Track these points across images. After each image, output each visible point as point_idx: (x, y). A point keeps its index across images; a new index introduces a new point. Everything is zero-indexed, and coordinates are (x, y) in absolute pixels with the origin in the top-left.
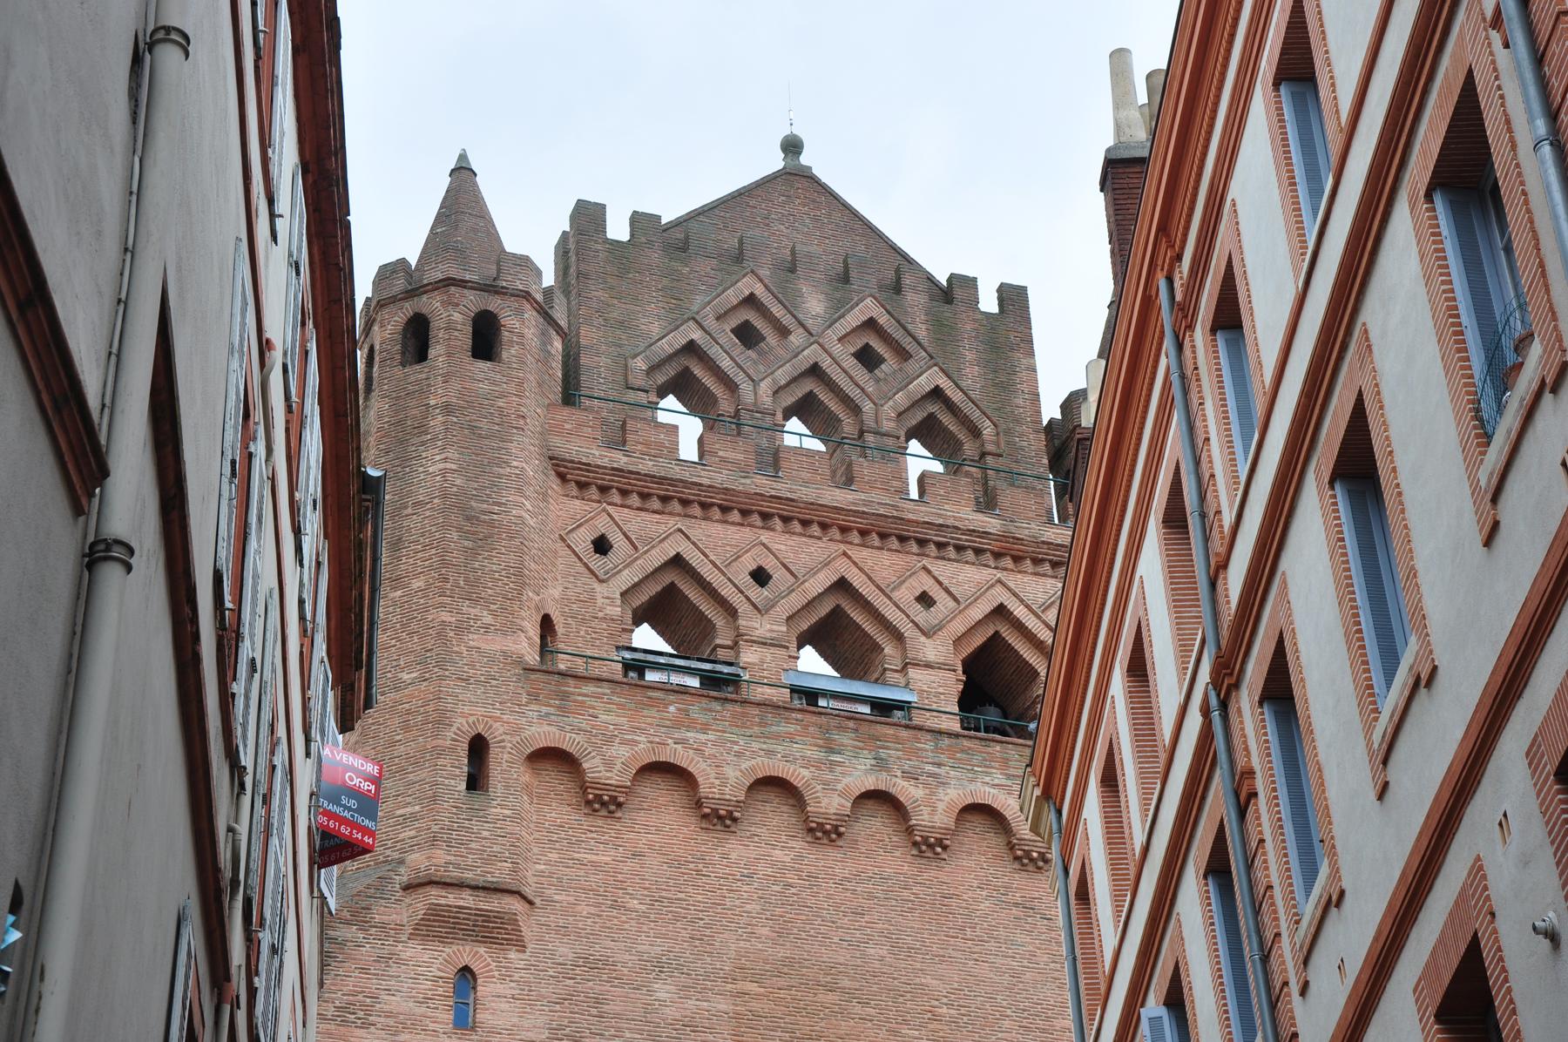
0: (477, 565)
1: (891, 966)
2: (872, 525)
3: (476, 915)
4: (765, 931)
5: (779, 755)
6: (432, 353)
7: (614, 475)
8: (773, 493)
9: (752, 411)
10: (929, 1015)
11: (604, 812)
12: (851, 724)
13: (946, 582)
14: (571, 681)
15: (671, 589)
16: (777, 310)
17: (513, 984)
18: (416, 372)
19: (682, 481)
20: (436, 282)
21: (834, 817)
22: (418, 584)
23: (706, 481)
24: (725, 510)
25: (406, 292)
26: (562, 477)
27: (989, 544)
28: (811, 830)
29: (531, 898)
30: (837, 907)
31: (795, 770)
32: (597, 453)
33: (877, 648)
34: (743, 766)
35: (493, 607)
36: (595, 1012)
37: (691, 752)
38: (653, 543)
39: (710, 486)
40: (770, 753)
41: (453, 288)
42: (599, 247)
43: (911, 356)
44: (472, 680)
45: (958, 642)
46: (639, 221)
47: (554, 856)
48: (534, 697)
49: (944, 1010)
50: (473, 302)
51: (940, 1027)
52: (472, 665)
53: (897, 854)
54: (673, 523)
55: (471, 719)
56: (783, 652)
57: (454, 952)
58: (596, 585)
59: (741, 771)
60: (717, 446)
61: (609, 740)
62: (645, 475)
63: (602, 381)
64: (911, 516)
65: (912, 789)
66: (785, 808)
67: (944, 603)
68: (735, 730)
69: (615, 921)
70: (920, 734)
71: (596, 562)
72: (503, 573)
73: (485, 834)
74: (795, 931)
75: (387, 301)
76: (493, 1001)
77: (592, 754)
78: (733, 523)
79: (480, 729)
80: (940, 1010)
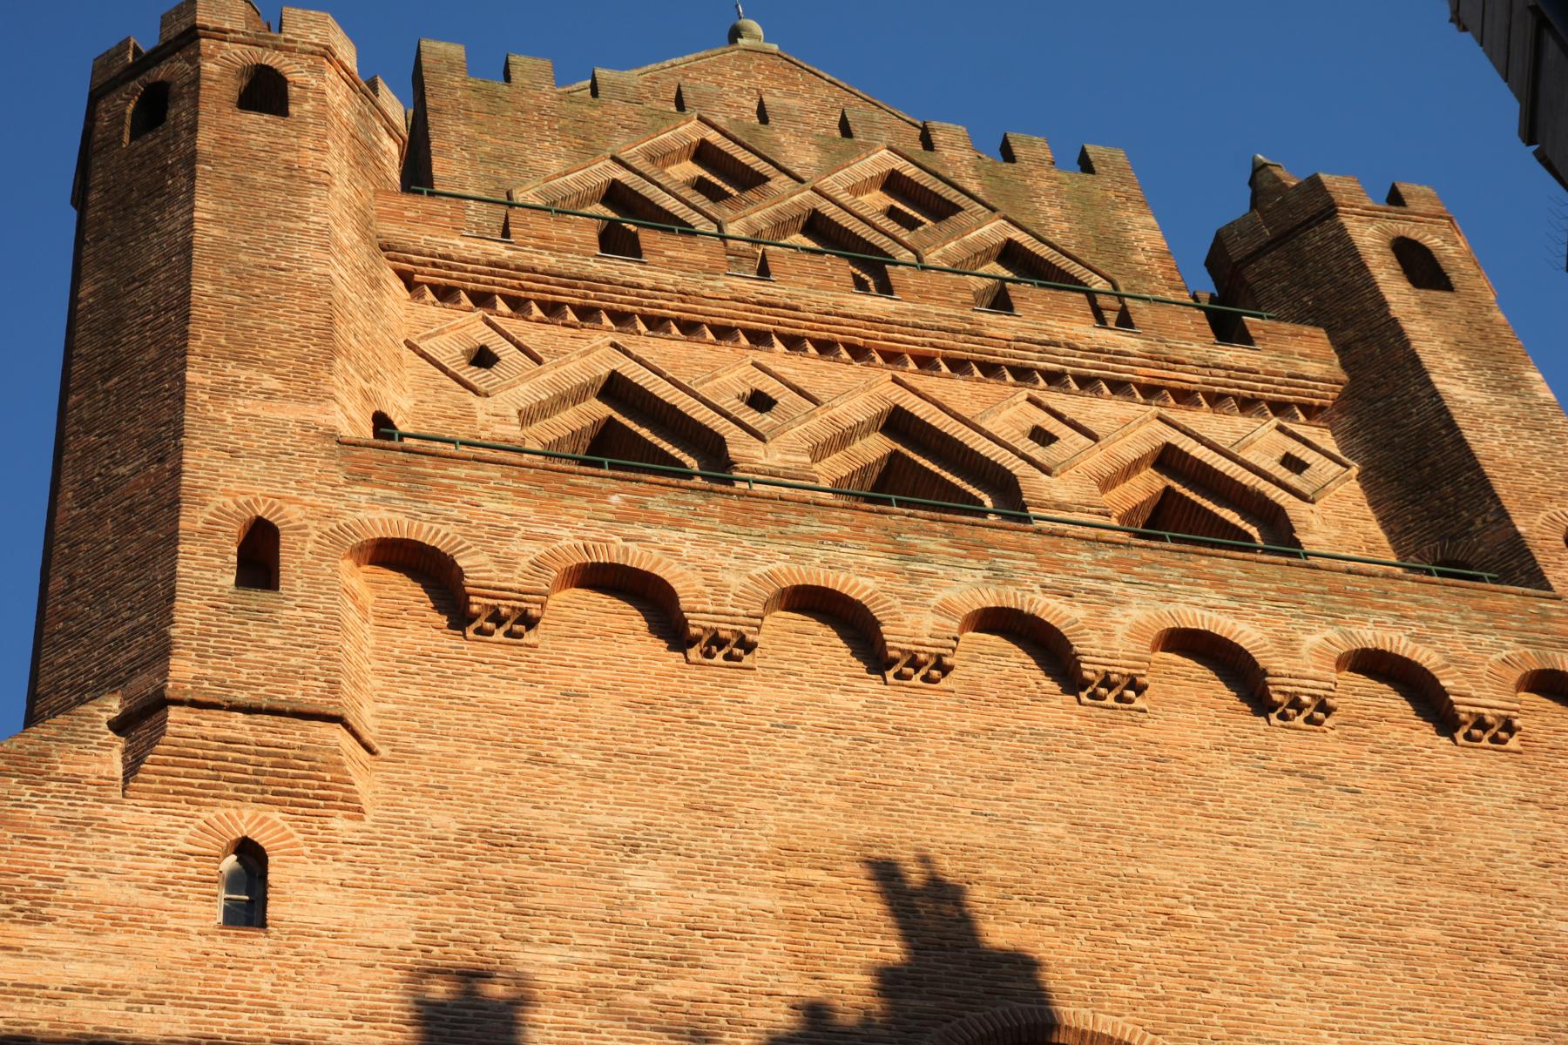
1: (1076, 850)
2: (932, 345)
3: (257, 753)
4: (829, 799)
5: (817, 561)
7: (492, 274)
8: (762, 297)
13: (1070, 415)
14: (425, 459)
17: (338, 865)
21: (933, 641)
31: (848, 579)
34: (753, 573)
36: (510, 906)
47: (413, 692)
49: (1190, 911)
52: (244, 434)
55: (242, 499)
61: (506, 533)
73: (272, 642)
74: (885, 799)
77: (474, 549)
79: (261, 511)
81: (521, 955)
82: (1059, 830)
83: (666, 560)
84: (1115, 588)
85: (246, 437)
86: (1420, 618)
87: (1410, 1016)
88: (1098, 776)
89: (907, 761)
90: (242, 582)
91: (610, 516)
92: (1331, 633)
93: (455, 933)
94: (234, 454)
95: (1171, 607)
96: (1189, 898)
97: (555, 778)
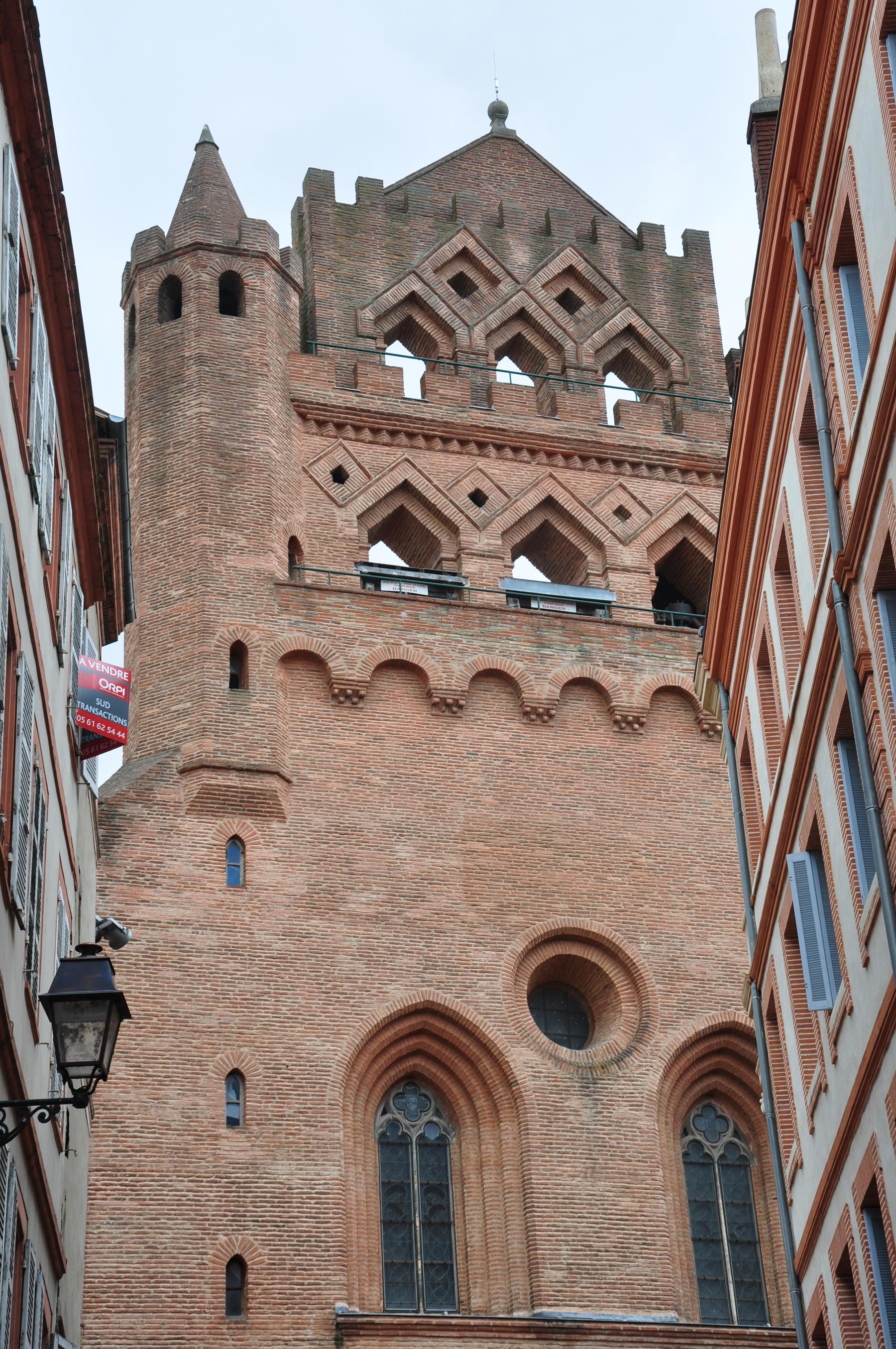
0: (231, 495)
3: (242, 792)
4: (489, 799)
6: (185, 310)
7: (348, 413)
9: (468, 353)
10: (631, 864)
11: (348, 704)
12: (559, 622)
13: (639, 497)
14: (316, 594)
15: (401, 512)
16: (488, 262)
17: (276, 849)
18: (172, 328)
19: (407, 417)
20: (186, 247)
22: (181, 514)
23: (428, 416)
24: (446, 440)
25: (161, 256)
26: (303, 417)
27: (677, 462)
28: (526, 714)
29: (288, 777)
30: (550, 777)
31: (511, 663)
32: (332, 394)
33: (581, 556)
34: (466, 661)
35: (246, 531)
37: (421, 650)
38: (383, 472)
39: (432, 421)
40: (489, 649)
41: (200, 252)
42: (329, 210)
43: (607, 299)
44: (231, 595)
45: (651, 548)
46: (364, 186)
47: (306, 742)
48: (285, 608)
49: (644, 860)
50: (218, 263)
51: (639, 873)
53: (601, 731)
54: (401, 453)
55: (231, 628)
56: (500, 562)
57: (225, 824)
58: (336, 510)
59: (465, 665)
60: (437, 385)
61: (350, 642)
62: (375, 413)
63: (335, 330)
64: (608, 441)
65: (612, 676)
66: (504, 696)
67: (638, 515)
68: (459, 630)
69: (361, 795)
70: (618, 629)
71: (335, 490)
72: (254, 502)
73: (247, 724)
74: (515, 798)
75: (144, 265)
76: (260, 863)
77: (337, 655)
78: (453, 452)
79: (239, 636)
80: (640, 860)
81: (351, 898)
83: (426, 656)
85: (232, 584)
87: (730, 916)
91: (401, 626)
96: (644, 851)
97: (368, 792)
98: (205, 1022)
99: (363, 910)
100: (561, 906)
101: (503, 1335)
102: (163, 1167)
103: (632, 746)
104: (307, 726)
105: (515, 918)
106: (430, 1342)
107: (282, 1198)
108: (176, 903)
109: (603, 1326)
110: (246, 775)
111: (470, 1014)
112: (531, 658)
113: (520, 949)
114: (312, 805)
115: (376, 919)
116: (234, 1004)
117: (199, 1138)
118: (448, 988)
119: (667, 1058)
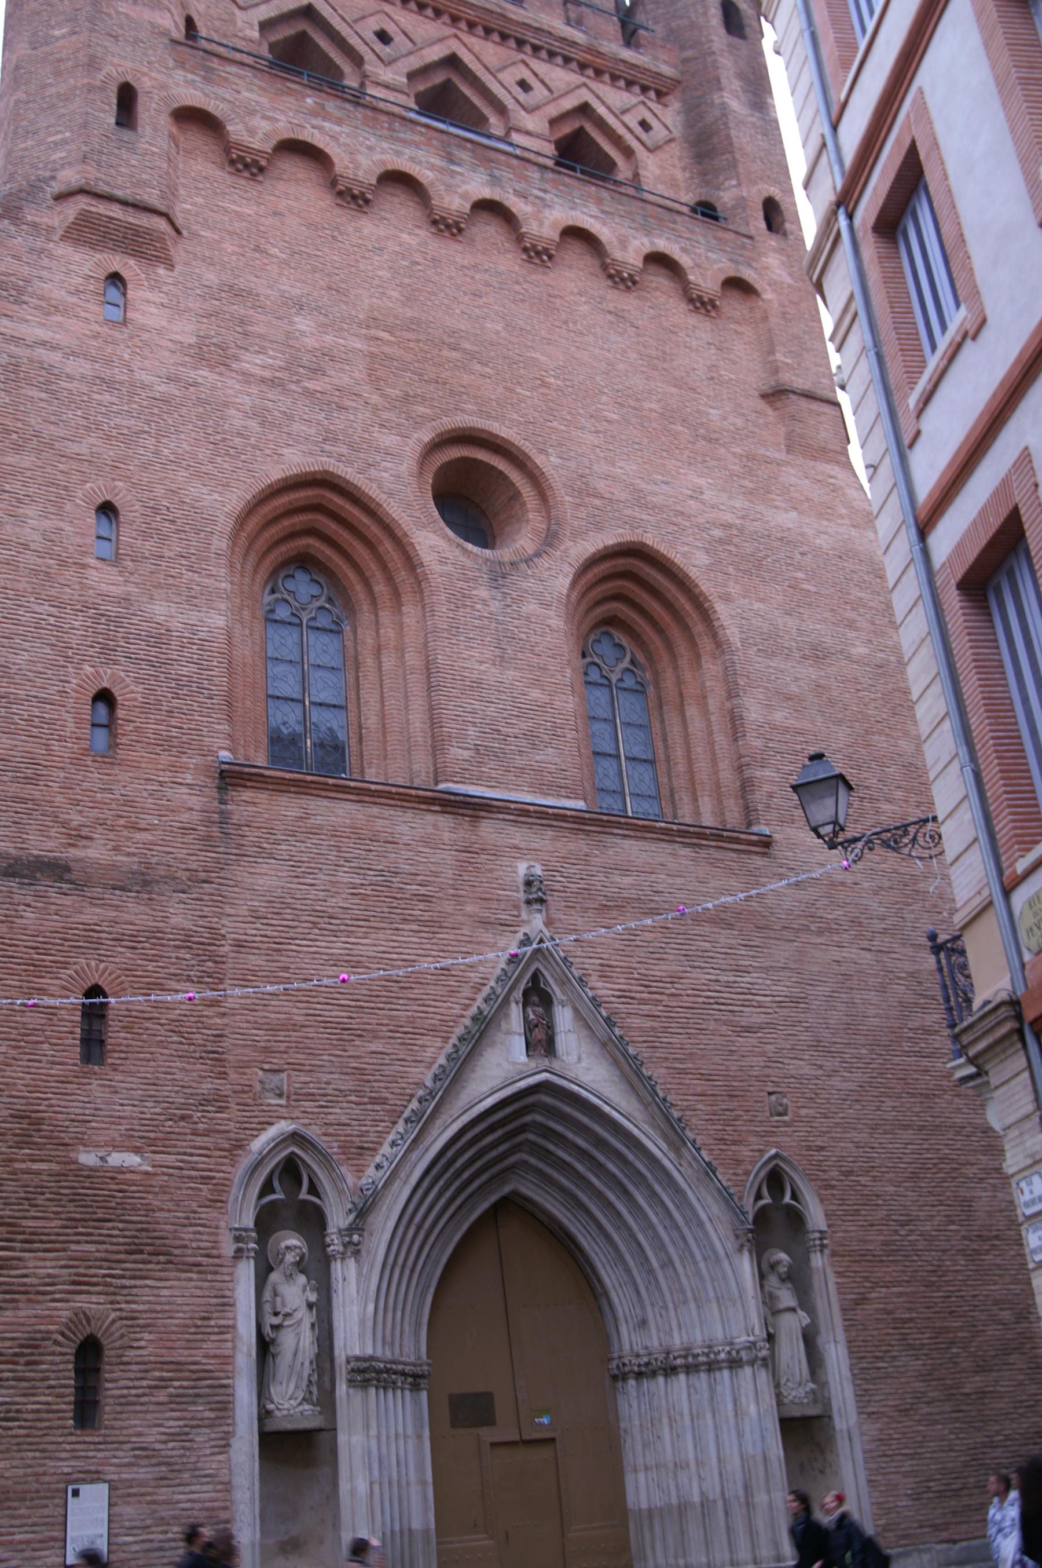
4: (395, 294)
11: (246, 174)
12: (469, 145)
13: (541, 76)
14: (215, 60)
15: (302, 38)
28: (435, 222)
30: (458, 288)
40: (398, 153)
45: (553, 122)
47: (199, 200)
48: (181, 65)
49: (552, 380)
52: (121, 27)
53: (509, 256)
55: (120, 69)
61: (252, 113)
64: (514, 17)
66: (411, 204)
67: (539, 93)
70: (528, 165)
73: (134, 162)
79: (129, 79)
82: (499, 327)
84: (547, 196)
86: (688, 239)
88: (523, 301)
89: (435, 278)
90: (118, 123)
92: (645, 240)
93: (214, 340)
94: (116, 37)
95: (573, 213)
98: (75, 448)
99: (258, 371)
100: (469, 407)
101: (405, 804)
102: (20, 586)
103: (540, 277)
104: (201, 186)
105: (421, 410)
106: (325, 802)
107: (160, 637)
108: (44, 325)
109: (512, 806)
110: (130, 209)
111: (373, 491)
112: (442, 170)
113: (426, 439)
114: (203, 261)
115: (273, 383)
116: (109, 437)
117: (63, 563)
118: (349, 462)
119: (577, 565)
